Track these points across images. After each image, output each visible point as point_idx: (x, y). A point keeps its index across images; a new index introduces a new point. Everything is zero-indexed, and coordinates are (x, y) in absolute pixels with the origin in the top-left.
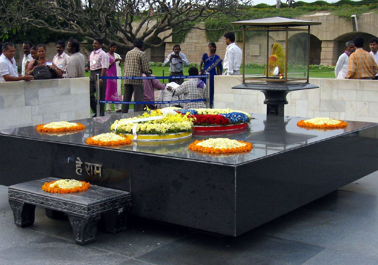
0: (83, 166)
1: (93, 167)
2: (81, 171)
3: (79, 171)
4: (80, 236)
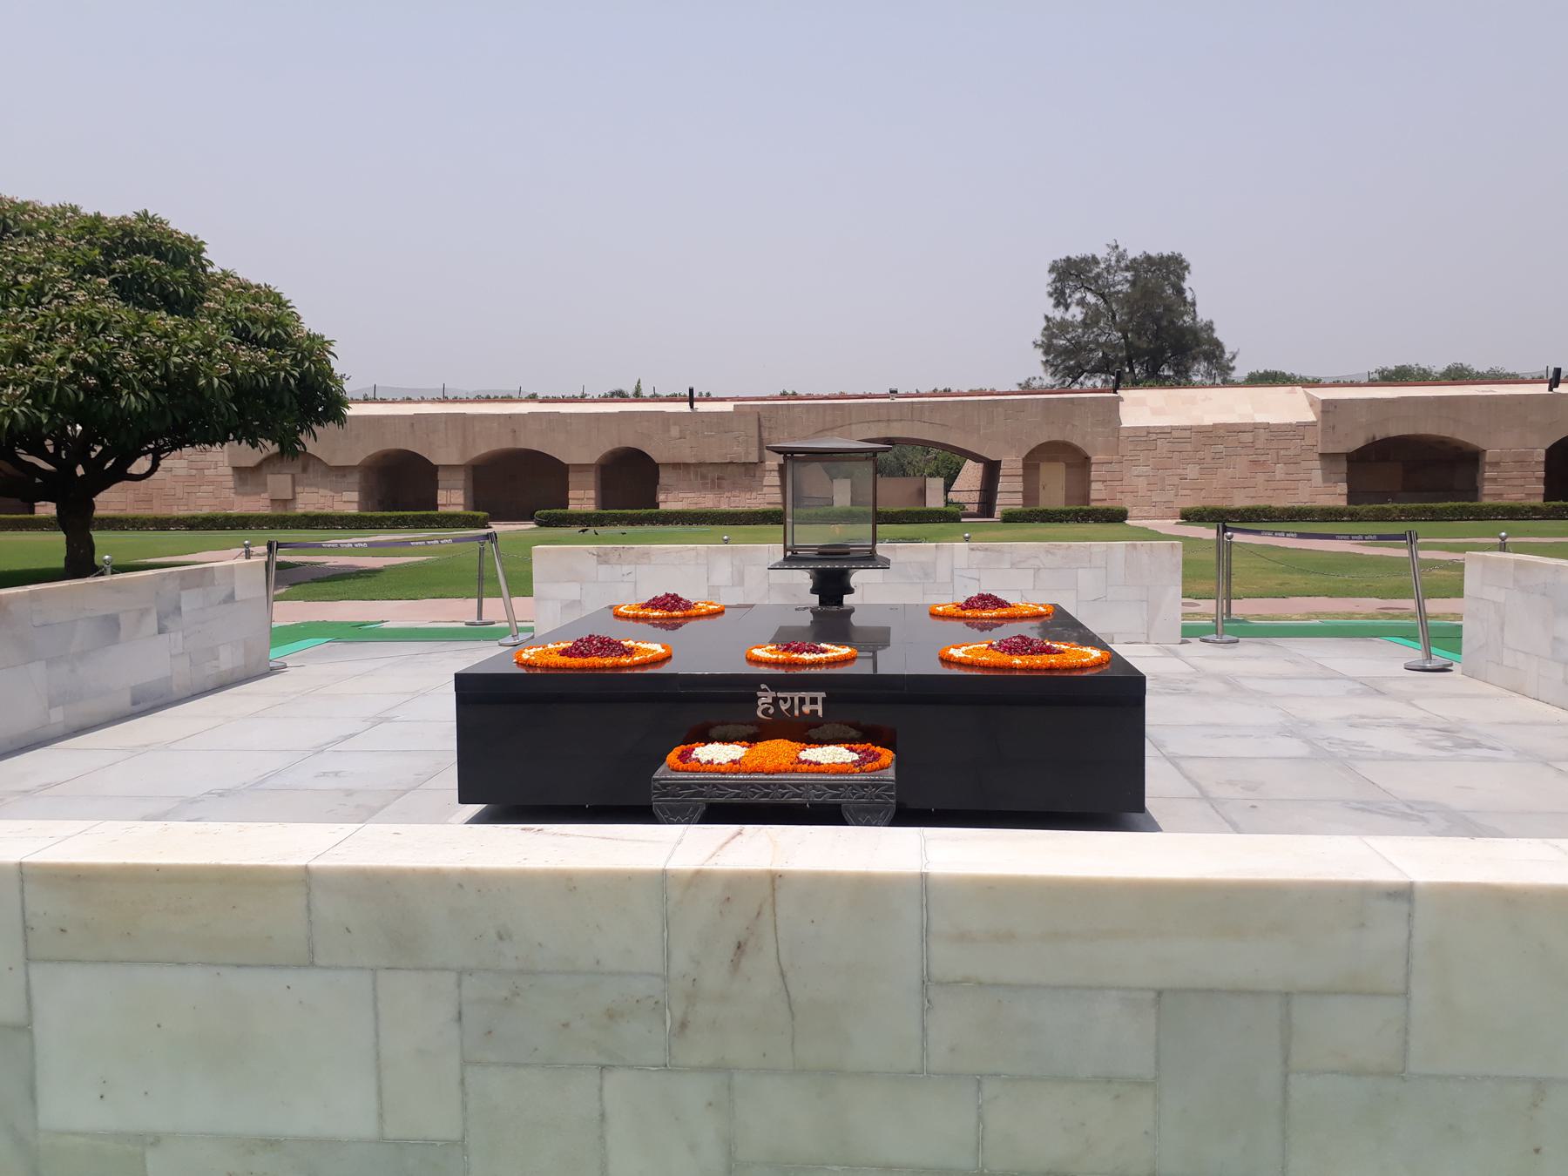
1: (802, 701)
2: (771, 711)
3: (765, 712)
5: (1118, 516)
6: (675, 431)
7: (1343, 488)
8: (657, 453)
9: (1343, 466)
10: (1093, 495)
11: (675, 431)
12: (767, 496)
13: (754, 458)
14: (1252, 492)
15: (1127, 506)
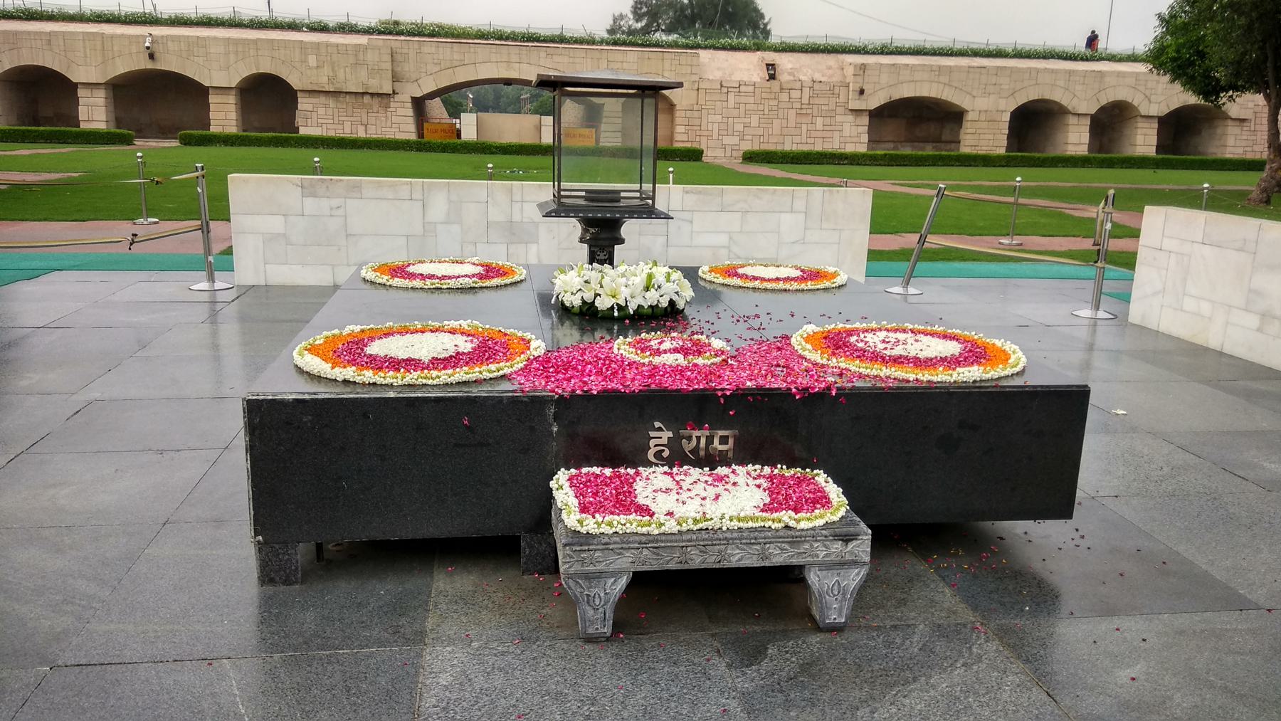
0: (674, 444)
1: (710, 440)
2: (666, 453)
4: (840, 615)
5: (694, 155)
6: (312, 60)
7: (865, 138)
8: (295, 81)
9: (865, 120)
10: (678, 137)
11: (312, 60)
12: (401, 125)
13: (387, 89)
14: (797, 139)
15: (703, 147)
